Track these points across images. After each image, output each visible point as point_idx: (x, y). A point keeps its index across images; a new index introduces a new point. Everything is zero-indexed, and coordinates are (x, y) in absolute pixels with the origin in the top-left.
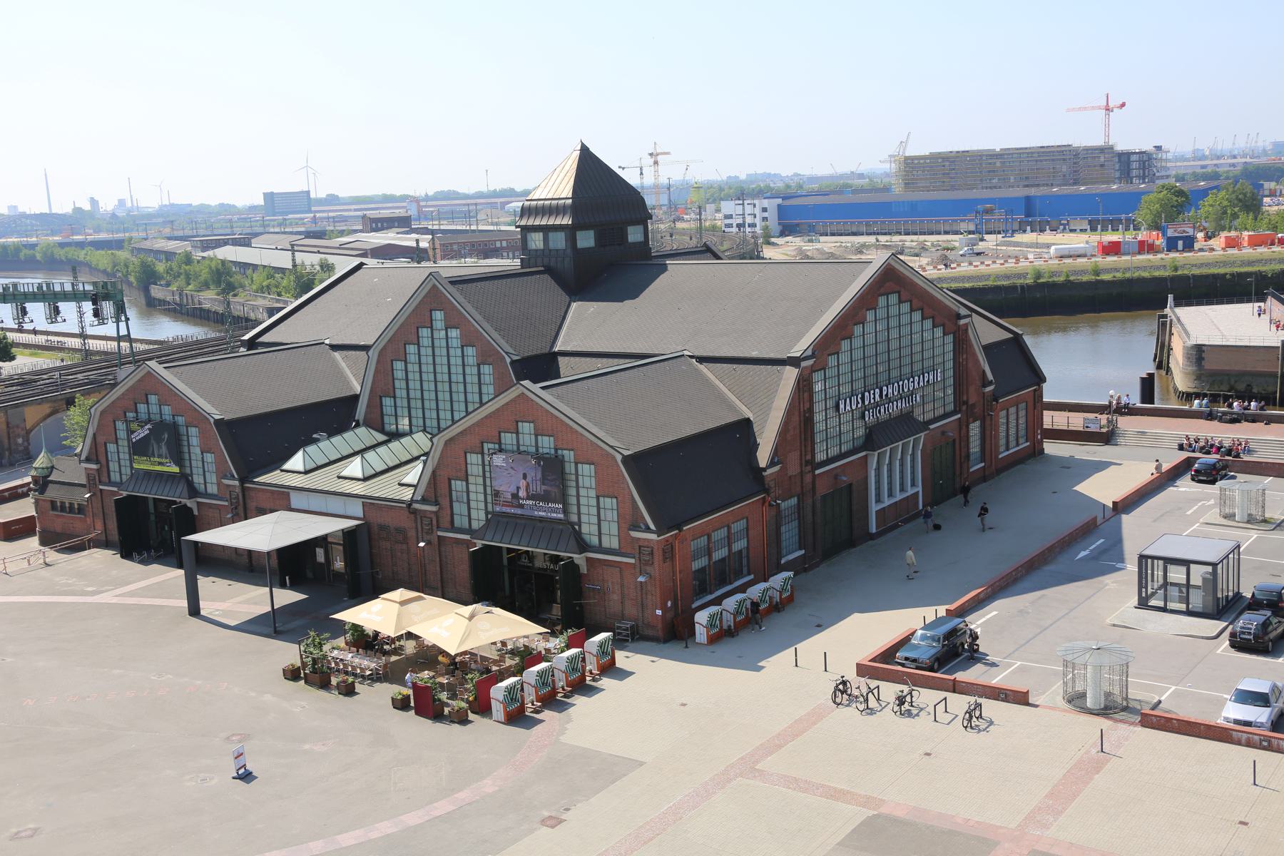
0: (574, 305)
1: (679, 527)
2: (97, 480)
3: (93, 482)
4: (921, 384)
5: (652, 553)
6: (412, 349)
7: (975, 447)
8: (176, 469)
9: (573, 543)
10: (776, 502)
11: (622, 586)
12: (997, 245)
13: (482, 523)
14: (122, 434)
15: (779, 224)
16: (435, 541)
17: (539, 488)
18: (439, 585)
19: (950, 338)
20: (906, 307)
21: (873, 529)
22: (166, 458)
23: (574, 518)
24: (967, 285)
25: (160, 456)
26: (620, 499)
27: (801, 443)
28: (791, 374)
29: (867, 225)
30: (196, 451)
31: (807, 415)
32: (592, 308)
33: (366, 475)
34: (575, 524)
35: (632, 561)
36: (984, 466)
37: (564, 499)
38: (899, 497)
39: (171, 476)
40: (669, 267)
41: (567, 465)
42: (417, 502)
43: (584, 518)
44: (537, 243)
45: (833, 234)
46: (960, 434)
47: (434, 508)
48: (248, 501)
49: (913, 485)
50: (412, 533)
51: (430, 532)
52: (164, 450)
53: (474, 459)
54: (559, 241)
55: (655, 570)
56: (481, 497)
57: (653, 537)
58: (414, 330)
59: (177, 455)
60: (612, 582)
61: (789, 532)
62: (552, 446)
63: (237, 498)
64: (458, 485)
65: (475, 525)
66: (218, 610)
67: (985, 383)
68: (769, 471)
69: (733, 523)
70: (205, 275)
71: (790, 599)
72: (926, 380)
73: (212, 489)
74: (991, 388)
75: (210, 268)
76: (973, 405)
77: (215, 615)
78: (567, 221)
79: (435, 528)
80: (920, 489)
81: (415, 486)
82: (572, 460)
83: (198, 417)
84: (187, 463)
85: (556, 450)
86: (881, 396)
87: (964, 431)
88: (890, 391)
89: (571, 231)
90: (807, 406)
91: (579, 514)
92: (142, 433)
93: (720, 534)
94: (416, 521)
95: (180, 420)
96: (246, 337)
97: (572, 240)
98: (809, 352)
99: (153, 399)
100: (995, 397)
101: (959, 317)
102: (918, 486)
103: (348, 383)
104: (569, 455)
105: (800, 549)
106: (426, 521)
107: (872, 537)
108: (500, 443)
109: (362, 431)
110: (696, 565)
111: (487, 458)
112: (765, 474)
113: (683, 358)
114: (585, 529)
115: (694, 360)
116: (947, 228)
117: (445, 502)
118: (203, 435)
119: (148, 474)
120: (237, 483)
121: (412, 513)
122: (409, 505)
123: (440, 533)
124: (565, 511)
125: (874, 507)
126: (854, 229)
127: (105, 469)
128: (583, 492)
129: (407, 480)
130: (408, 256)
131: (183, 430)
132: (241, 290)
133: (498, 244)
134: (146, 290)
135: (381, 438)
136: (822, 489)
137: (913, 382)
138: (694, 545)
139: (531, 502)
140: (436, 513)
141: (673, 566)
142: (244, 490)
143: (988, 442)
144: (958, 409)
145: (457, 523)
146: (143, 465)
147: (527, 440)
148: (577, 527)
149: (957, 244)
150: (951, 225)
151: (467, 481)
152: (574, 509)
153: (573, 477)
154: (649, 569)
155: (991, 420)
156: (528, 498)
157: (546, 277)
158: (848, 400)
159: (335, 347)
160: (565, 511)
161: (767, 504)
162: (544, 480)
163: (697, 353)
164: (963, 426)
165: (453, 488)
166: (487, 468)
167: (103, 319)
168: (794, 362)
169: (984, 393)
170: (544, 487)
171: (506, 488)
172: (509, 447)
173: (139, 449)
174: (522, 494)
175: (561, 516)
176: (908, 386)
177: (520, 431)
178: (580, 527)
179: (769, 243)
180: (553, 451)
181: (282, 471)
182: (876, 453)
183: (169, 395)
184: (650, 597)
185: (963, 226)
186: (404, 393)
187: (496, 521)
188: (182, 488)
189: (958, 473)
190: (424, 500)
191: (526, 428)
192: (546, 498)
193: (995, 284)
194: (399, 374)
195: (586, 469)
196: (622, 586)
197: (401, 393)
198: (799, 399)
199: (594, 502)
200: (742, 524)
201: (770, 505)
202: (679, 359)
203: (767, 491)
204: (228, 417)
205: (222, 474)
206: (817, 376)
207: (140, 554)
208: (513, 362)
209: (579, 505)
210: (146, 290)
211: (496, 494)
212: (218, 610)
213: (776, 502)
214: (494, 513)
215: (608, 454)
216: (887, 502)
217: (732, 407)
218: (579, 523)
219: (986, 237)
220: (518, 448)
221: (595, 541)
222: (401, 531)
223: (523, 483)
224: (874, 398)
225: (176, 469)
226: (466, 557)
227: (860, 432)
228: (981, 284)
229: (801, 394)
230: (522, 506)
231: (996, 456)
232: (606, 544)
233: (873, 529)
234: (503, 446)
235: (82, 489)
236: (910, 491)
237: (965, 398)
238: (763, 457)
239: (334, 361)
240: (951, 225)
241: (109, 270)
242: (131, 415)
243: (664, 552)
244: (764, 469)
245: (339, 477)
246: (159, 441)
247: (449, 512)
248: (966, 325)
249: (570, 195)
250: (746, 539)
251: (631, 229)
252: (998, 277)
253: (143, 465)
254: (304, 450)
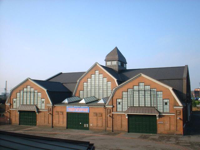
5: (180, 112)
13: (126, 110)
35: (174, 115)
60: (167, 121)
62: (149, 88)
63: (51, 109)
65: (124, 110)
85: (151, 89)
106: (109, 110)
123: (113, 113)
145: (118, 110)
148: (156, 108)
151: (122, 99)
165: (118, 101)
177: (140, 85)
178: (157, 107)
197: (85, 90)
232: (165, 111)
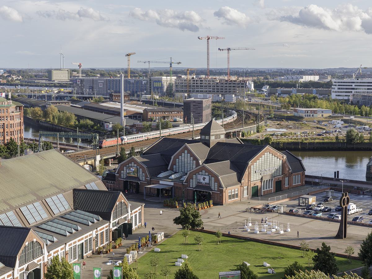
6: (180, 157)
16: (187, 189)
47: (187, 184)
48: (151, 182)
49: (272, 187)
53: (194, 176)
67: (289, 170)
76: (286, 174)
87: (284, 179)
93: (233, 190)
114: (212, 187)
117: (189, 183)
128: (212, 182)
138: (229, 191)
145: (191, 187)
187: (197, 186)
194: (177, 161)
205: (146, 176)
221: (214, 189)
232: (215, 190)
236: (270, 189)
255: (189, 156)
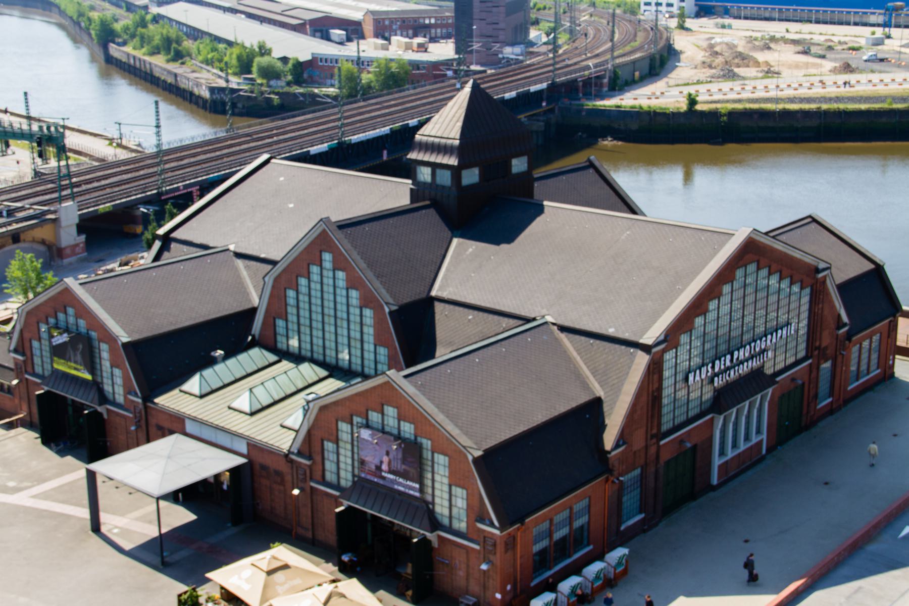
0: (455, 241)
1: (521, 520)
2: (23, 370)
3: (19, 370)
4: (774, 340)
5: (495, 545)
6: (303, 281)
7: (824, 385)
8: (89, 377)
9: (426, 521)
10: (618, 479)
11: (468, 566)
12: (901, 46)
14: (45, 336)
15: (696, 5)
16: (308, 490)
17: (400, 467)
18: (310, 527)
19: (807, 291)
20: (764, 272)
21: (715, 481)
22: (81, 365)
23: (429, 498)
24: (863, 107)
25: (76, 362)
26: (469, 491)
27: (647, 420)
28: (642, 360)
29: (780, 10)
30: (106, 364)
31: (655, 394)
32: (472, 247)
33: (253, 410)
34: (430, 503)
35: (477, 547)
36: (832, 401)
37: (420, 480)
38: (743, 446)
39: (84, 381)
40: (546, 210)
41: (425, 452)
42: (293, 453)
43: (437, 500)
44: (426, 176)
45: (746, 18)
46: (810, 375)
48: (150, 418)
49: (758, 431)
50: (288, 478)
51: (304, 480)
52: (79, 358)
53: (344, 427)
54: (445, 178)
55: (497, 559)
56: (349, 461)
57: (497, 532)
58: (305, 266)
59: (92, 364)
61: (630, 500)
63: (140, 412)
64: (329, 446)
66: (116, 527)
67: (840, 324)
68: (613, 453)
69: (576, 503)
70: (157, 40)
71: (625, 572)
72: (779, 335)
73: (120, 399)
74: (846, 329)
75: (162, 34)
76: (826, 348)
77: (115, 534)
78: (453, 161)
79: (308, 478)
80: (764, 436)
81: (297, 431)
82: (429, 447)
83: (109, 338)
84: (99, 373)
86: (732, 360)
88: (742, 354)
89: (456, 172)
90: (656, 385)
91: (433, 495)
92: (61, 339)
94: (292, 468)
95: (94, 334)
96: (161, 232)
97: (456, 172)
98: (662, 337)
99: (71, 311)
100: (849, 336)
101: (818, 271)
102: (762, 434)
103: (246, 294)
104: (427, 443)
105: (641, 512)
106: (300, 472)
107: (714, 488)
108: (367, 419)
109: (255, 352)
110: (537, 548)
111: (355, 430)
112: (609, 456)
113: (545, 326)
114: (438, 509)
115: (556, 328)
116: (857, 20)
117: (318, 458)
118: (112, 351)
119: (66, 375)
120: (140, 401)
121: (289, 462)
122: (286, 456)
123: (313, 484)
124: (421, 490)
125: (717, 461)
126: (767, 15)
127: (29, 362)
129: (289, 423)
130: (343, 27)
131: (96, 343)
132: (188, 59)
133: (427, 22)
134: (105, 48)
135: (272, 358)
136: (665, 456)
137: (766, 341)
138: (535, 531)
139: (391, 476)
140: (310, 467)
141: (515, 555)
142: (146, 407)
143: (837, 378)
144: (809, 355)
146: (61, 366)
147: (391, 422)
148: (431, 506)
149: (863, 42)
150: (861, 17)
152: (430, 491)
153: (430, 463)
154: (492, 557)
155: (843, 358)
156: (390, 472)
157: (432, 212)
158: (698, 372)
159: (239, 255)
160: (421, 490)
161: (610, 482)
162: (404, 460)
163: (560, 322)
164: (814, 370)
166: (355, 443)
167: (46, 159)
168: (646, 348)
169: (837, 335)
170: (404, 467)
171: (372, 460)
172: (375, 425)
173: (59, 351)
174: (385, 467)
175: (417, 494)
176: (759, 345)
179: (681, 27)
180: (413, 438)
181: (181, 391)
182: (722, 417)
183: (83, 311)
184: (491, 581)
185: (873, 19)
186: (295, 319)
187: (361, 486)
188: (93, 394)
189: (805, 411)
190: (300, 453)
191: (391, 411)
192: (405, 475)
193: (891, 107)
194: (291, 301)
195: (441, 459)
196: (468, 566)
197: (292, 318)
198: (649, 380)
199: (446, 488)
200: (585, 502)
201: (613, 482)
202: (541, 328)
203: (609, 471)
204: (137, 337)
205: (128, 391)
206: (669, 356)
207: (57, 445)
208: (391, 313)
209: (433, 488)
210: (105, 48)
211: (362, 462)
212: (116, 527)
213: (618, 479)
214: (359, 477)
215: (461, 452)
216: (730, 454)
217: (585, 386)
218: (433, 503)
219: (894, 32)
220: (383, 428)
221: (446, 521)
222: (278, 473)
223: (386, 459)
224: (725, 364)
225: (89, 377)
226: (333, 518)
227: (708, 395)
228: (876, 106)
229: (651, 376)
230: (384, 478)
231: (845, 389)
233: (715, 481)
234: (370, 423)
235: (12, 373)
236: (754, 440)
237: (817, 344)
238: (609, 438)
239: (236, 270)
240: (861, 17)
241: (75, 18)
242: (52, 321)
243: (506, 544)
244: (609, 452)
245: (230, 408)
246: (75, 349)
247: (321, 468)
248: (825, 277)
249: (458, 136)
250: (587, 516)
251: (515, 162)
252: (895, 99)
253: (61, 366)
254: (201, 375)
255: (341, 283)
